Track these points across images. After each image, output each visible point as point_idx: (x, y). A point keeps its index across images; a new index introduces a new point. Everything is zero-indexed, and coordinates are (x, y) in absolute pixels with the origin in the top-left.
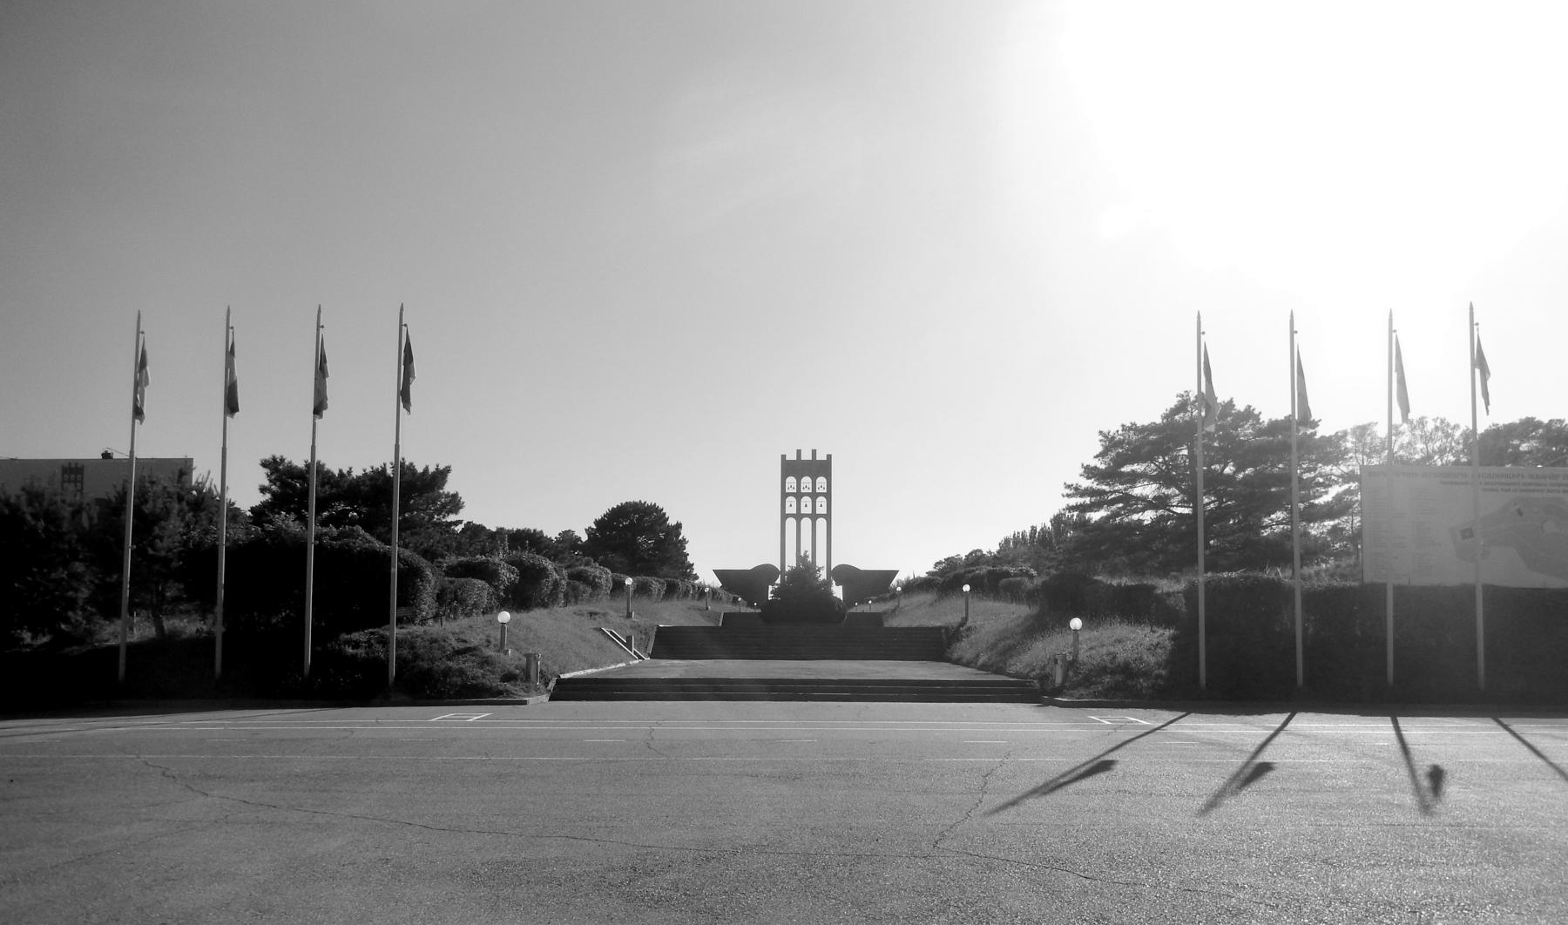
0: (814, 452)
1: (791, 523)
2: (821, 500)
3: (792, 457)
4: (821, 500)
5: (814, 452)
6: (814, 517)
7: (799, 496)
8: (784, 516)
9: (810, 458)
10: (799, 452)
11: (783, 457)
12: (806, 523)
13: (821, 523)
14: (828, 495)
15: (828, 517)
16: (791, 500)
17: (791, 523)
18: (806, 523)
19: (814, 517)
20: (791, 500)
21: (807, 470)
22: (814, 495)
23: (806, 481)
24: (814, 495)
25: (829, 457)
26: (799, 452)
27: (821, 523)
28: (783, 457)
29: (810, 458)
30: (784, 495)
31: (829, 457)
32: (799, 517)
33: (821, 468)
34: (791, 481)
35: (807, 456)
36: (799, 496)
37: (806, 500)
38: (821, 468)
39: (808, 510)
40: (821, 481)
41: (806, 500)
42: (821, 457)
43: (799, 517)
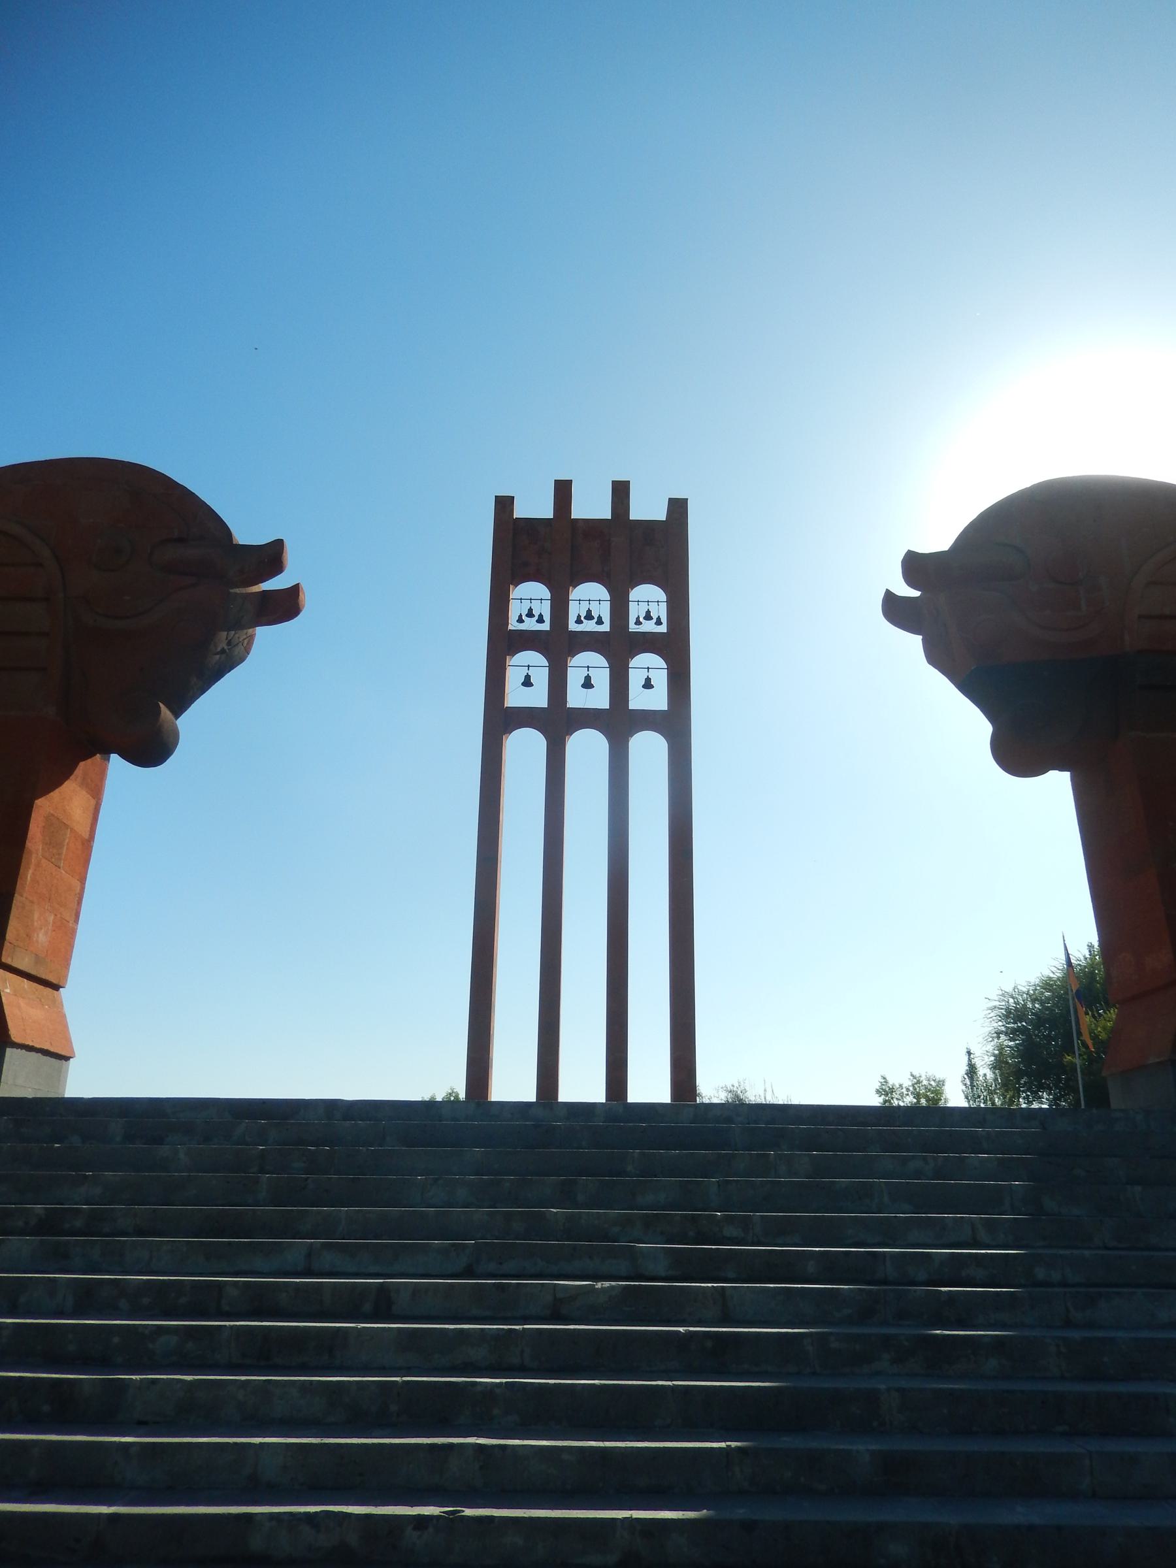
0: (621, 491)
1: (525, 749)
2: (648, 666)
3: (536, 505)
4: (648, 666)
5: (621, 491)
6: (618, 722)
7: (558, 644)
8: (500, 720)
9: (603, 511)
10: (563, 490)
11: (504, 505)
12: (587, 749)
13: (648, 751)
14: (674, 646)
15: (674, 724)
16: (529, 665)
17: (525, 749)
18: (587, 749)
19: (618, 722)
20: (529, 665)
22: (620, 645)
23: (590, 600)
24: (620, 645)
25: (678, 508)
26: (563, 490)
27: (648, 751)
28: (504, 505)
29: (607, 515)
30: (503, 642)
31: (678, 508)
32: (557, 722)
34: (530, 600)
35: (592, 505)
36: (558, 644)
37: (589, 665)
39: (599, 698)
40: (648, 602)
41: (589, 665)
42: (647, 507)
43: (557, 722)
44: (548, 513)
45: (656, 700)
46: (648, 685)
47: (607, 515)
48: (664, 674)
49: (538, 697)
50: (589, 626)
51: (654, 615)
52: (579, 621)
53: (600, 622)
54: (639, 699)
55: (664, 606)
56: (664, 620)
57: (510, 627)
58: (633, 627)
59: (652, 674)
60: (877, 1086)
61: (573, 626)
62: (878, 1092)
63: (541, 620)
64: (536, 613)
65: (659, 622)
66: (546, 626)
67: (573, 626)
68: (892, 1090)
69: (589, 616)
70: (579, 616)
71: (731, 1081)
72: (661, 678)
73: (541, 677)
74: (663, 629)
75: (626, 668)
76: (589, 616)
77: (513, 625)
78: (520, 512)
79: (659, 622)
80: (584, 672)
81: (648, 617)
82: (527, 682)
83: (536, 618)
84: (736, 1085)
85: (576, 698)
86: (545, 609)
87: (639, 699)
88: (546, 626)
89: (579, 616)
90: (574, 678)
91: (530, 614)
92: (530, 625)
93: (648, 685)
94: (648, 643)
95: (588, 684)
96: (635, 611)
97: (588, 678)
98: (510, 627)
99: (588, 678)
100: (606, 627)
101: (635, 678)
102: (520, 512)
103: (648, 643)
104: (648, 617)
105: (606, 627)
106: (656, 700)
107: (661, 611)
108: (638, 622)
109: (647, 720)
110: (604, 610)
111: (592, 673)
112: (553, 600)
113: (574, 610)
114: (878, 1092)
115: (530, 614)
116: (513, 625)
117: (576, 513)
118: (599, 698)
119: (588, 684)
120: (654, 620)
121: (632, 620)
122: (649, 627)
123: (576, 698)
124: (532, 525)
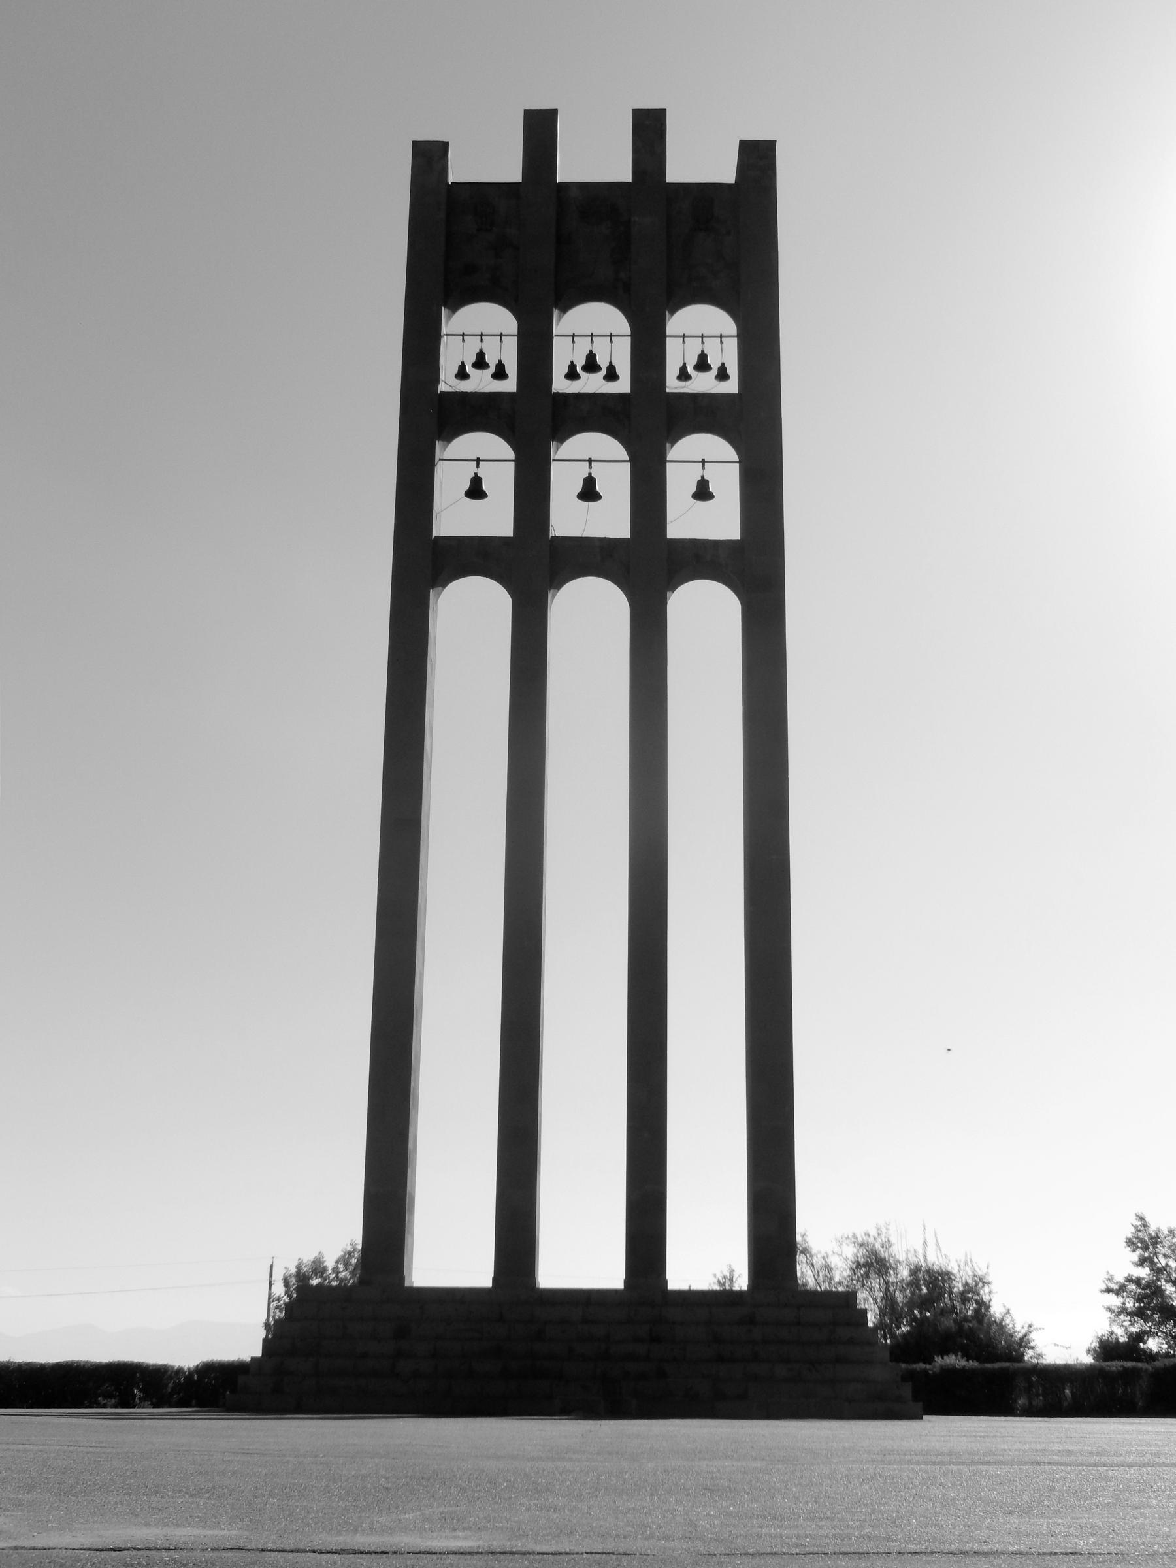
0: (649, 129)
3: (488, 157)
5: (649, 129)
6: (648, 566)
7: (534, 418)
8: (424, 562)
10: (540, 130)
11: (429, 158)
12: (589, 618)
14: (751, 419)
15: (754, 567)
18: (589, 618)
19: (648, 566)
21: (598, 299)
22: (648, 419)
24: (648, 419)
25: (758, 158)
26: (540, 130)
28: (429, 158)
29: (624, 174)
30: (430, 416)
31: (758, 158)
32: (532, 564)
33: (703, 238)
35: (594, 156)
36: (534, 418)
38: (703, 238)
39: (611, 519)
40: (701, 336)
42: (700, 158)
43: (532, 564)
44: (514, 174)
45: (720, 521)
46: (703, 492)
47: (624, 174)
48: (734, 471)
49: (495, 518)
50: (592, 384)
51: (714, 361)
52: (572, 375)
53: (612, 375)
54: (686, 521)
55: (732, 346)
56: (733, 370)
57: (442, 387)
58: (673, 384)
59: (710, 473)
60: (1129, 1232)
61: (560, 384)
62: (1130, 1243)
63: (500, 373)
64: (491, 360)
65: (723, 375)
66: (509, 385)
67: (560, 384)
68: (1155, 1240)
69: (591, 365)
70: (572, 366)
71: (865, 1225)
72: (727, 481)
73: (501, 481)
74: (731, 386)
75: (662, 461)
76: (591, 365)
77: (448, 383)
78: (459, 172)
79: (723, 375)
80: (583, 471)
81: (702, 365)
82: (476, 491)
83: (492, 369)
84: (873, 1233)
85: (568, 518)
86: (508, 353)
87: (686, 521)
88: (509, 385)
89: (572, 366)
90: (564, 480)
91: (480, 363)
92: (481, 382)
93: (703, 492)
94: (702, 414)
95: (589, 492)
96: (677, 354)
97: (590, 482)
98: (442, 387)
99: (590, 482)
100: (623, 386)
101: (679, 482)
102: (459, 172)
103: (702, 414)
104: (702, 365)
105: (623, 386)
106: (720, 521)
107: (727, 354)
108: (684, 375)
109: (701, 559)
110: (621, 354)
111: (597, 471)
112: (522, 336)
113: (563, 354)
114: (1130, 1243)
115: (480, 363)
116: (448, 383)
117: (563, 175)
118: (611, 519)
119: (589, 492)
120: (715, 372)
121: (672, 371)
122: (704, 383)
123: (568, 518)
124: (482, 195)
